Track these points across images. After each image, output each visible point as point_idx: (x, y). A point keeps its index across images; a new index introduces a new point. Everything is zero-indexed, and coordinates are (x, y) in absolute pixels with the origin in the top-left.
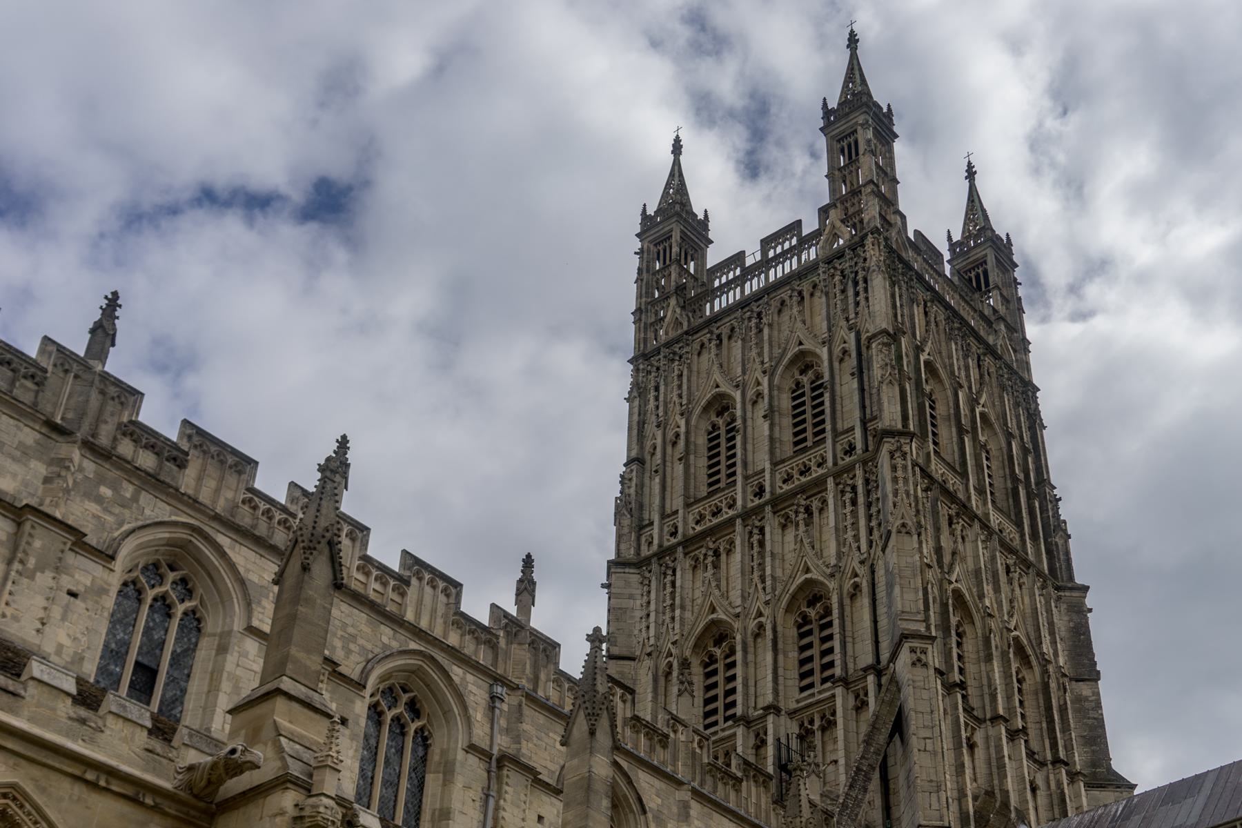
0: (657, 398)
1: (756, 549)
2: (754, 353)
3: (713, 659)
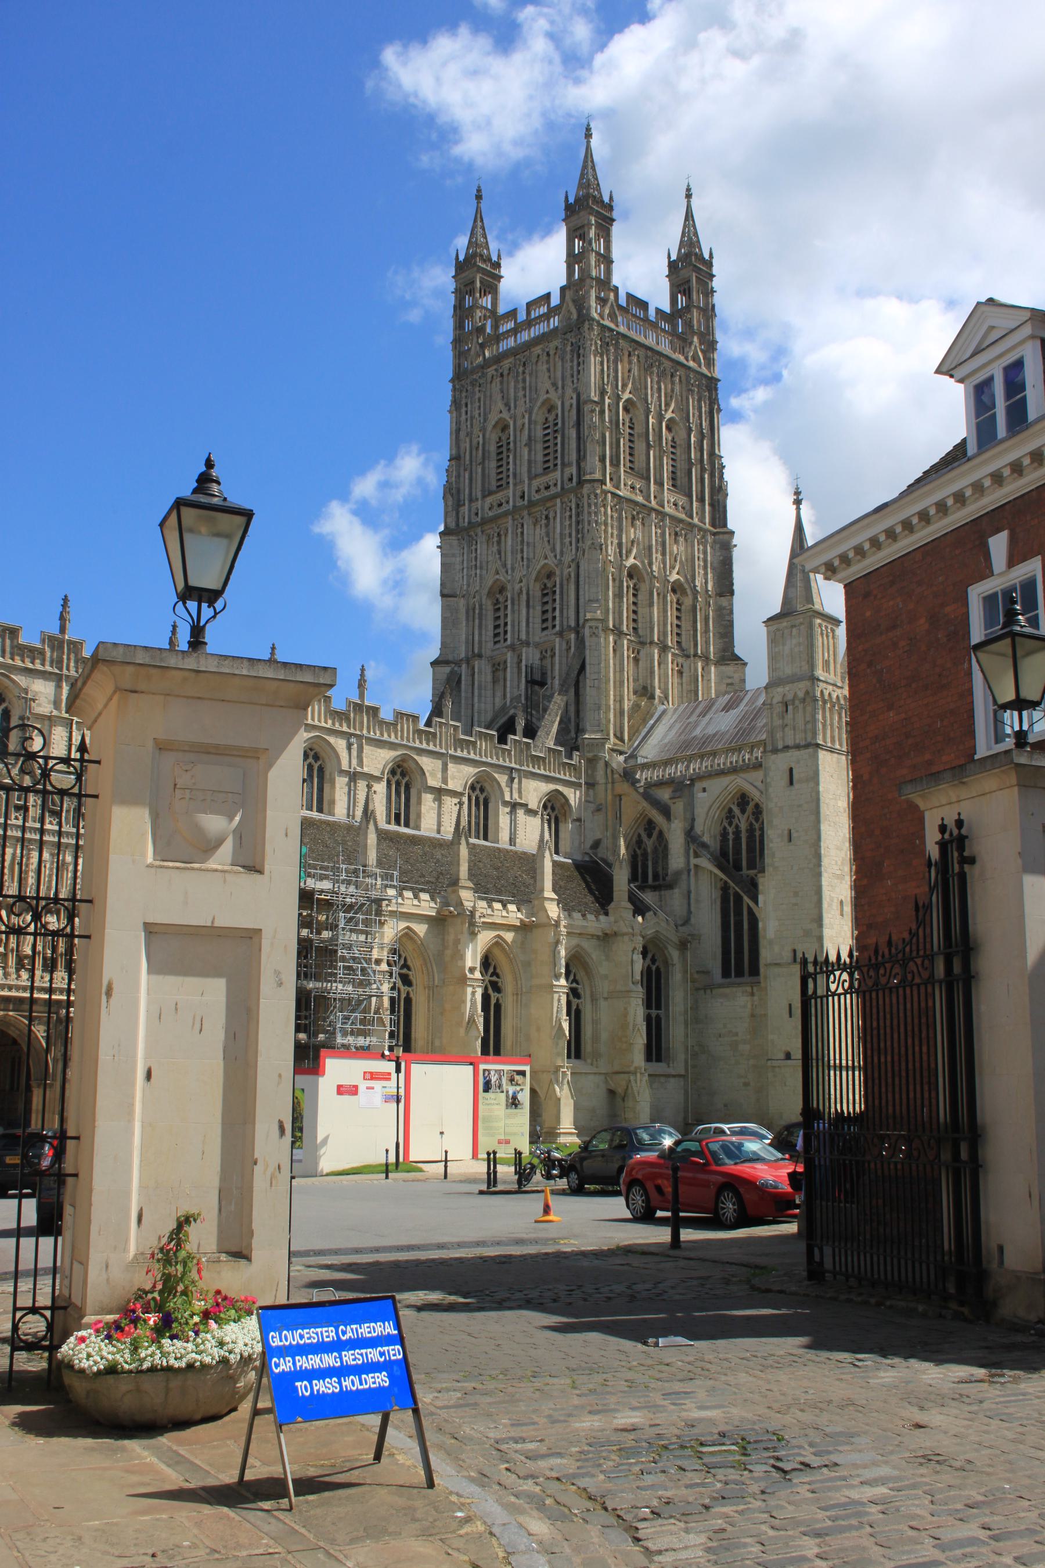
2: (521, 394)
3: (498, 602)
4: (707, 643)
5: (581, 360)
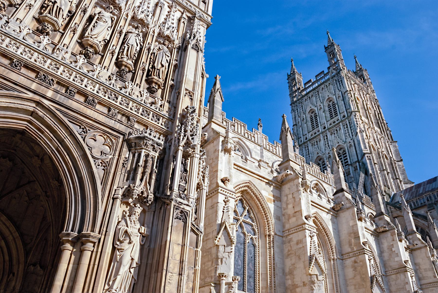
0: (298, 112)
1: (326, 140)
2: (318, 99)
4: (399, 176)
5: (340, 82)
